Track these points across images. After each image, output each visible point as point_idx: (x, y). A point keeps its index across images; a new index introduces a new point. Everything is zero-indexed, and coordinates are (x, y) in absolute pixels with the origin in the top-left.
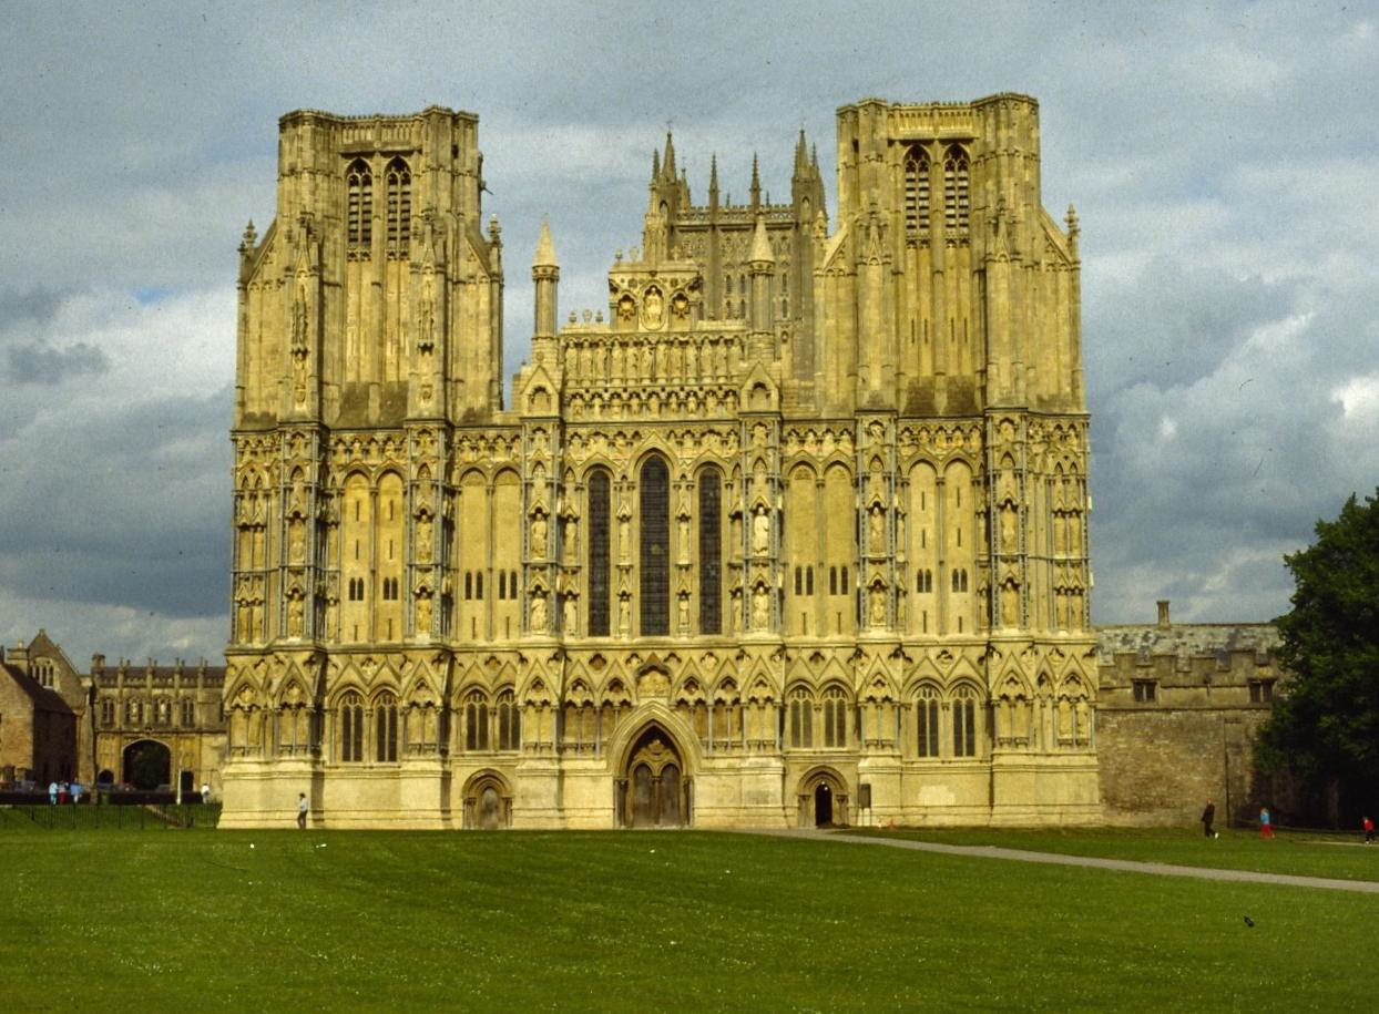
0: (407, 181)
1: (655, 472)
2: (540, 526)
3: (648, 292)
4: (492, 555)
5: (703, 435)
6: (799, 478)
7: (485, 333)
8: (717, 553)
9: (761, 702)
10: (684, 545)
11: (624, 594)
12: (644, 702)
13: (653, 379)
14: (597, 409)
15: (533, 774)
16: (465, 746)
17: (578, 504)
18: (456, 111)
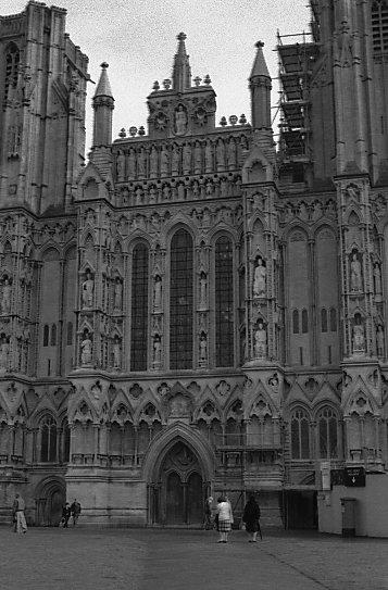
0: (17, 60)
1: (182, 242)
2: (89, 284)
3: (177, 110)
4: (62, 311)
5: (218, 210)
6: (295, 240)
7: (62, 150)
8: (230, 302)
9: (262, 420)
10: (204, 298)
11: (157, 336)
12: (171, 421)
13: (181, 173)
14: (138, 198)
15: (78, 480)
16: (39, 458)
17: (126, 270)
18: (48, 5)
